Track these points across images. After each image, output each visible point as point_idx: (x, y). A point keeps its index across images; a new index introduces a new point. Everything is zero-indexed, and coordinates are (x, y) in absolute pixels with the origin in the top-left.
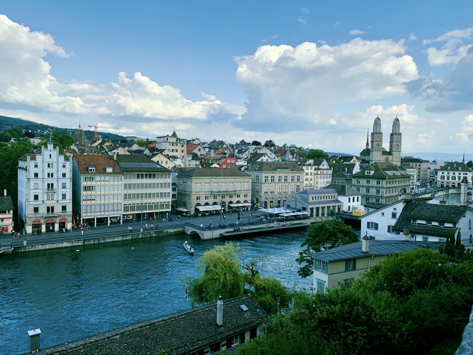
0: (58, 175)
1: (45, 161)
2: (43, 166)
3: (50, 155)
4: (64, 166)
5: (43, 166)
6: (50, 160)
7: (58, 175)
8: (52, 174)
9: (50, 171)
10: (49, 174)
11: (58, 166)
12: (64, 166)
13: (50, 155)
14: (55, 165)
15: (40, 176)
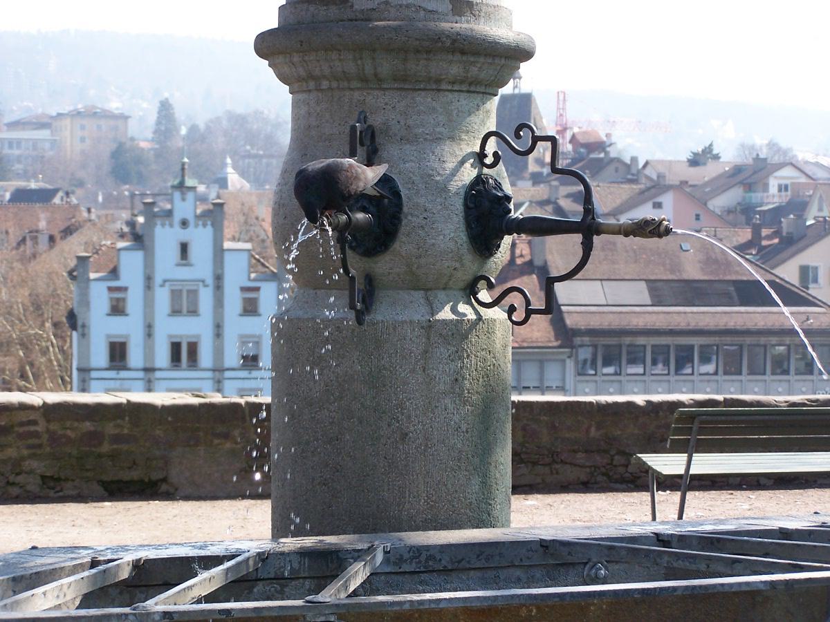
0: (219, 352)
1: (158, 279)
2: (149, 304)
3: (184, 248)
4: (251, 308)
5: (149, 304)
6: (184, 273)
7: (219, 352)
8: (193, 349)
9: (185, 328)
10: (176, 348)
11: (219, 302)
12: (251, 308)
13: (184, 248)
14: (206, 298)
15: (135, 357)
